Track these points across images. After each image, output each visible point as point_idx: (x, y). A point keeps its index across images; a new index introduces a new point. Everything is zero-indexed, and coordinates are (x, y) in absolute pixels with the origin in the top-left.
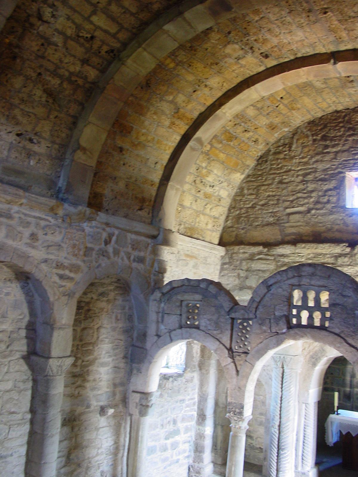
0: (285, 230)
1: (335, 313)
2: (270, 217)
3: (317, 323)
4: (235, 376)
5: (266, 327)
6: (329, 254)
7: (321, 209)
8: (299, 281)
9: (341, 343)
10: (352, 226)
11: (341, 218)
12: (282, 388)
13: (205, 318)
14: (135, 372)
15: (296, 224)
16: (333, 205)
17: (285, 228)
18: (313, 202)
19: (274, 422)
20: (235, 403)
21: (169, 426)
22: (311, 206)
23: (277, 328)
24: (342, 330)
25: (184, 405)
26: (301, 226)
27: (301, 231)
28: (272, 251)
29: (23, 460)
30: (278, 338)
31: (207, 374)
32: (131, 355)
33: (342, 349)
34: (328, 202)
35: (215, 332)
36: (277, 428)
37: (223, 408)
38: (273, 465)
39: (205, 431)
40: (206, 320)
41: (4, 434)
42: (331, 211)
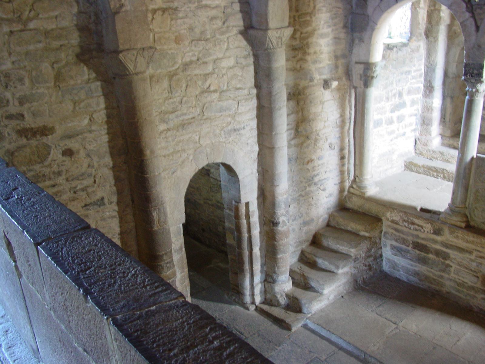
14: (357, 41)
21: (395, 98)
25: (410, 77)
29: (255, 133)
31: (435, 41)
32: (352, 24)
37: (453, 78)
39: (432, 103)
41: (234, 109)
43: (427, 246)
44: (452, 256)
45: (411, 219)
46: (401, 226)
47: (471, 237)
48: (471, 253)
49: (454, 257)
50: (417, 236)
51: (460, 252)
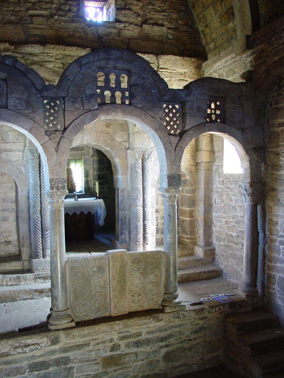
0: (28, 30)
1: (138, 92)
2: (11, 15)
3: (119, 101)
4: (54, 152)
5: (79, 104)
6: (77, 56)
7: (64, 16)
8: (106, 64)
9: (145, 115)
10: (90, 35)
11: (81, 27)
12: (40, 177)
13: (13, 97)
15: (39, 27)
16: (74, 14)
17: (29, 29)
18: (55, 8)
19: (36, 208)
20: (56, 179)
22: (54, 12)
23: (89, 106)
24: (144, 105)
26: (45, 29)
27: (45, 33)
28: (20, 48)
30: (93, 114)
33: (146, 120)
34: (70, 10)
35: (27, 112)
36: (39, 213)
38: (39, 246)
40: (14, 99)
42: (72, 19)
43: (46, 362)
44: (72, 357)
45: (23, 341)
46: (13, 355)
47: (86, 330)
48: (88, 345)
49: (74, 357)
50: (34, 357)
51: (80, 349)
